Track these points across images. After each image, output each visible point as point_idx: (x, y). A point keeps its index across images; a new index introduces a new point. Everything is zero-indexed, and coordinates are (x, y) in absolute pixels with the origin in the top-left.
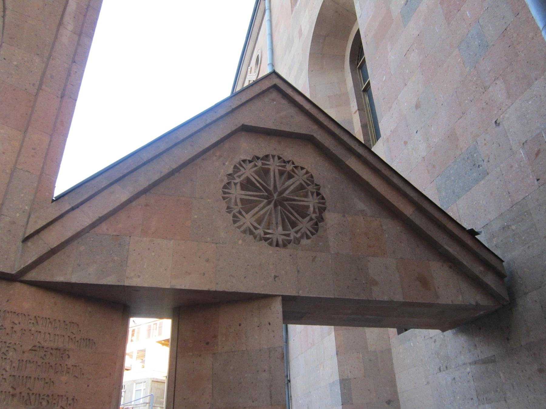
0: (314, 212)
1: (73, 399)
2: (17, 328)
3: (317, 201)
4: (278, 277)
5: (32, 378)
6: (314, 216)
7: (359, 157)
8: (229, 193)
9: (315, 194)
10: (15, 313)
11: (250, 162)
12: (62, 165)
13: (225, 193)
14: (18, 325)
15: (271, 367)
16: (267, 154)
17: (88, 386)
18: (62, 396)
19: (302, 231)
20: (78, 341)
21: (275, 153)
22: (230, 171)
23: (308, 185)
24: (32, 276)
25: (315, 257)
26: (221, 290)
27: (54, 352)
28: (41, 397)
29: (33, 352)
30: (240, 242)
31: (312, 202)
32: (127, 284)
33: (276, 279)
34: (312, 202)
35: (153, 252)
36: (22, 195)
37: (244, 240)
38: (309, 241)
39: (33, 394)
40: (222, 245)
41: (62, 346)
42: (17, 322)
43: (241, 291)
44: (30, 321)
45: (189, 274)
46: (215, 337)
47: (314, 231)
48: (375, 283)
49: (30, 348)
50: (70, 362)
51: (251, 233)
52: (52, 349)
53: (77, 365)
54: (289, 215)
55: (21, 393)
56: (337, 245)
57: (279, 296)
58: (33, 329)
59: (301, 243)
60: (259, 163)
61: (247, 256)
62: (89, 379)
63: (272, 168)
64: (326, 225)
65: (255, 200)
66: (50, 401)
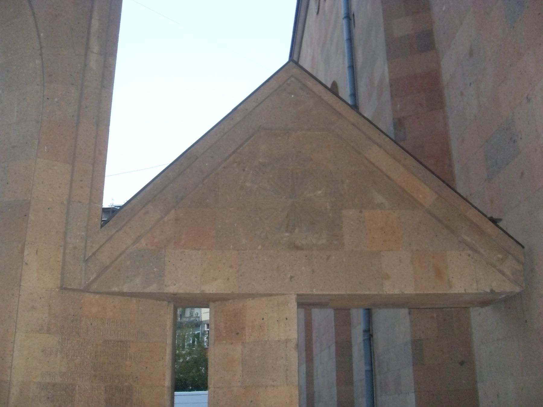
4: (294, 277)
12: (105, 192)
15: (287, 355)
24: (95, 287)
30: (260, 247)
32: (165, 291)
33: (292, 279)
36: (78, 224)
45: (216, 280)
46: (243, 328)
61: (266, 259)
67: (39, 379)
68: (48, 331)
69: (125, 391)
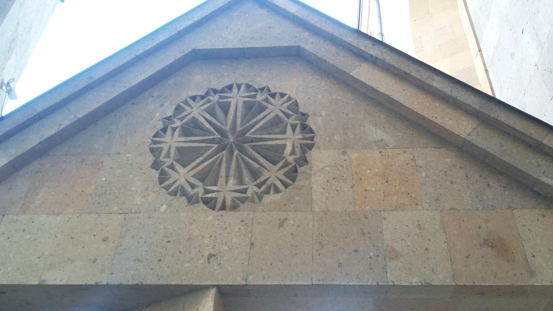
0: (293, 153)
3: (300, 136)
4: (215, 255)
6: (291, 159)
7: (374, 61)
8: (162, 142)
9: (298, 129)
11: (202, 97)
13: (155, 143)
16: (230, 83)
19: (269, 182)
21: (241, 81)
22: (169, 113)
23: (288, 116)
25: (286, 219)
26: (116, 283)
31: (290, 140)
34: (290, 140)
35: (29, 233)
37: (169, 205)
38: (278, 196)
40: (133, 215)
43: (149, 283)
45: (72, 261)
47: (288, 181)
48: (395, 255)
51: (184, 193)
54: (250, 161)
56: (327, 198)
57: (213, 286)
59: (263, 200)
60: (215, 98)
63: (233, 101)
64: (311, 168)
65: (199, 147)
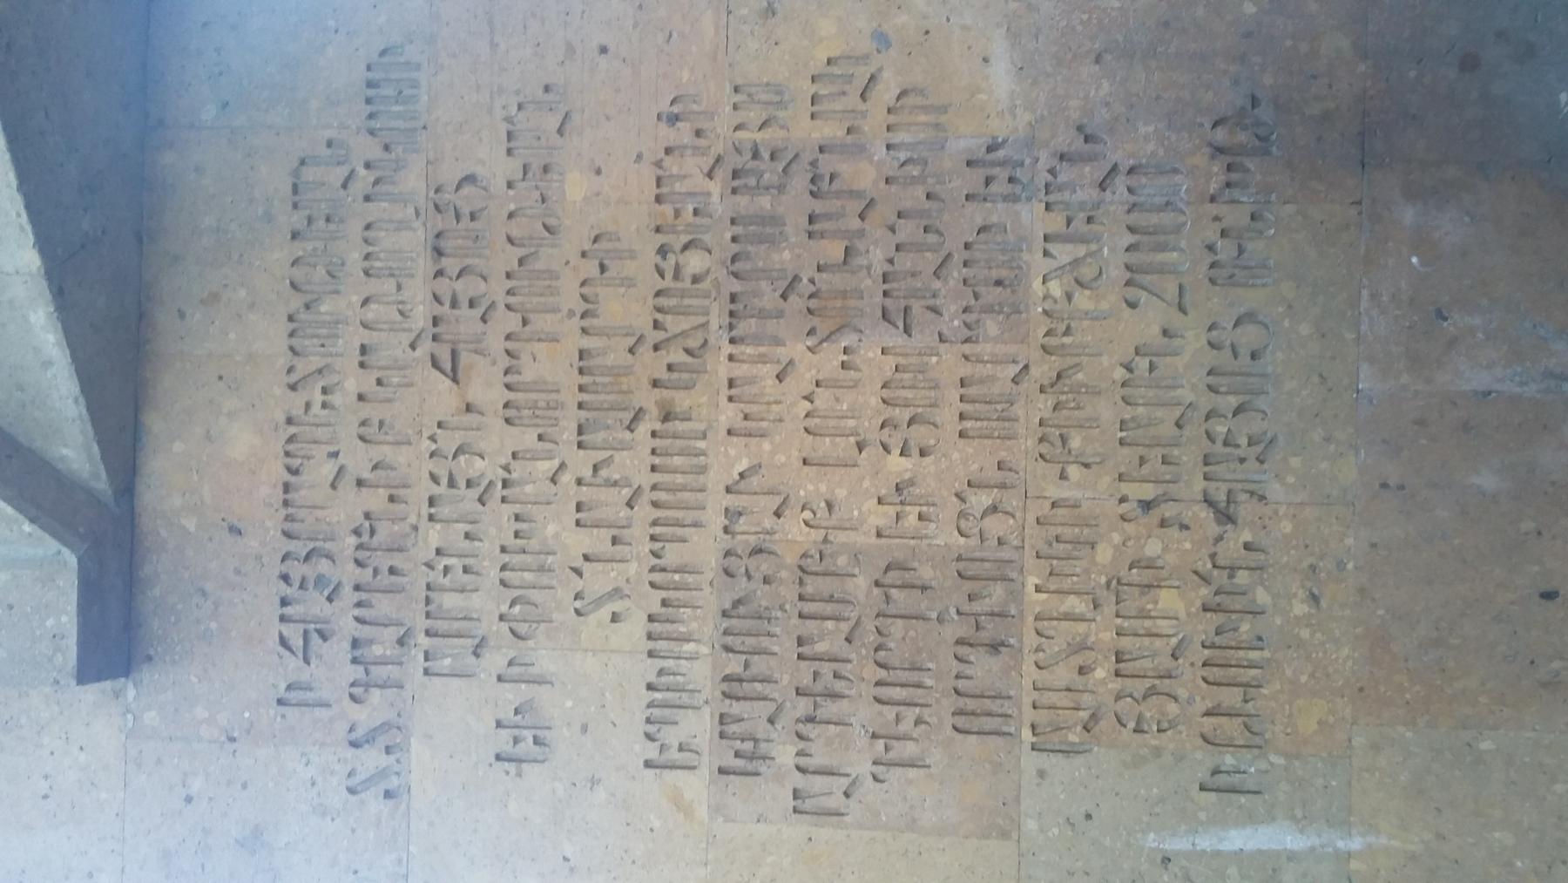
1: (674, 119)
2: (358, 460)
5: (587, 343)
10: (287, 488)
14: (341, 460)
17: (604, 50)
18: (659, 182)
20: (387, 148)
27: (451, 265)
28: (668, 282)
29: (464, 358)
39: (657, 325)
41: (416, 224)
42: (328, 469)
44: (316, 408)
49: (448, 382)
50: (496, 167)
52: (439, 273)
53: (503, 128)
55: (655, 384)
58: (352, 385)
62: (570, 49)
66: (685, 239)
67: (695, 786)
68: (388, 736)
69: (765, 202)
